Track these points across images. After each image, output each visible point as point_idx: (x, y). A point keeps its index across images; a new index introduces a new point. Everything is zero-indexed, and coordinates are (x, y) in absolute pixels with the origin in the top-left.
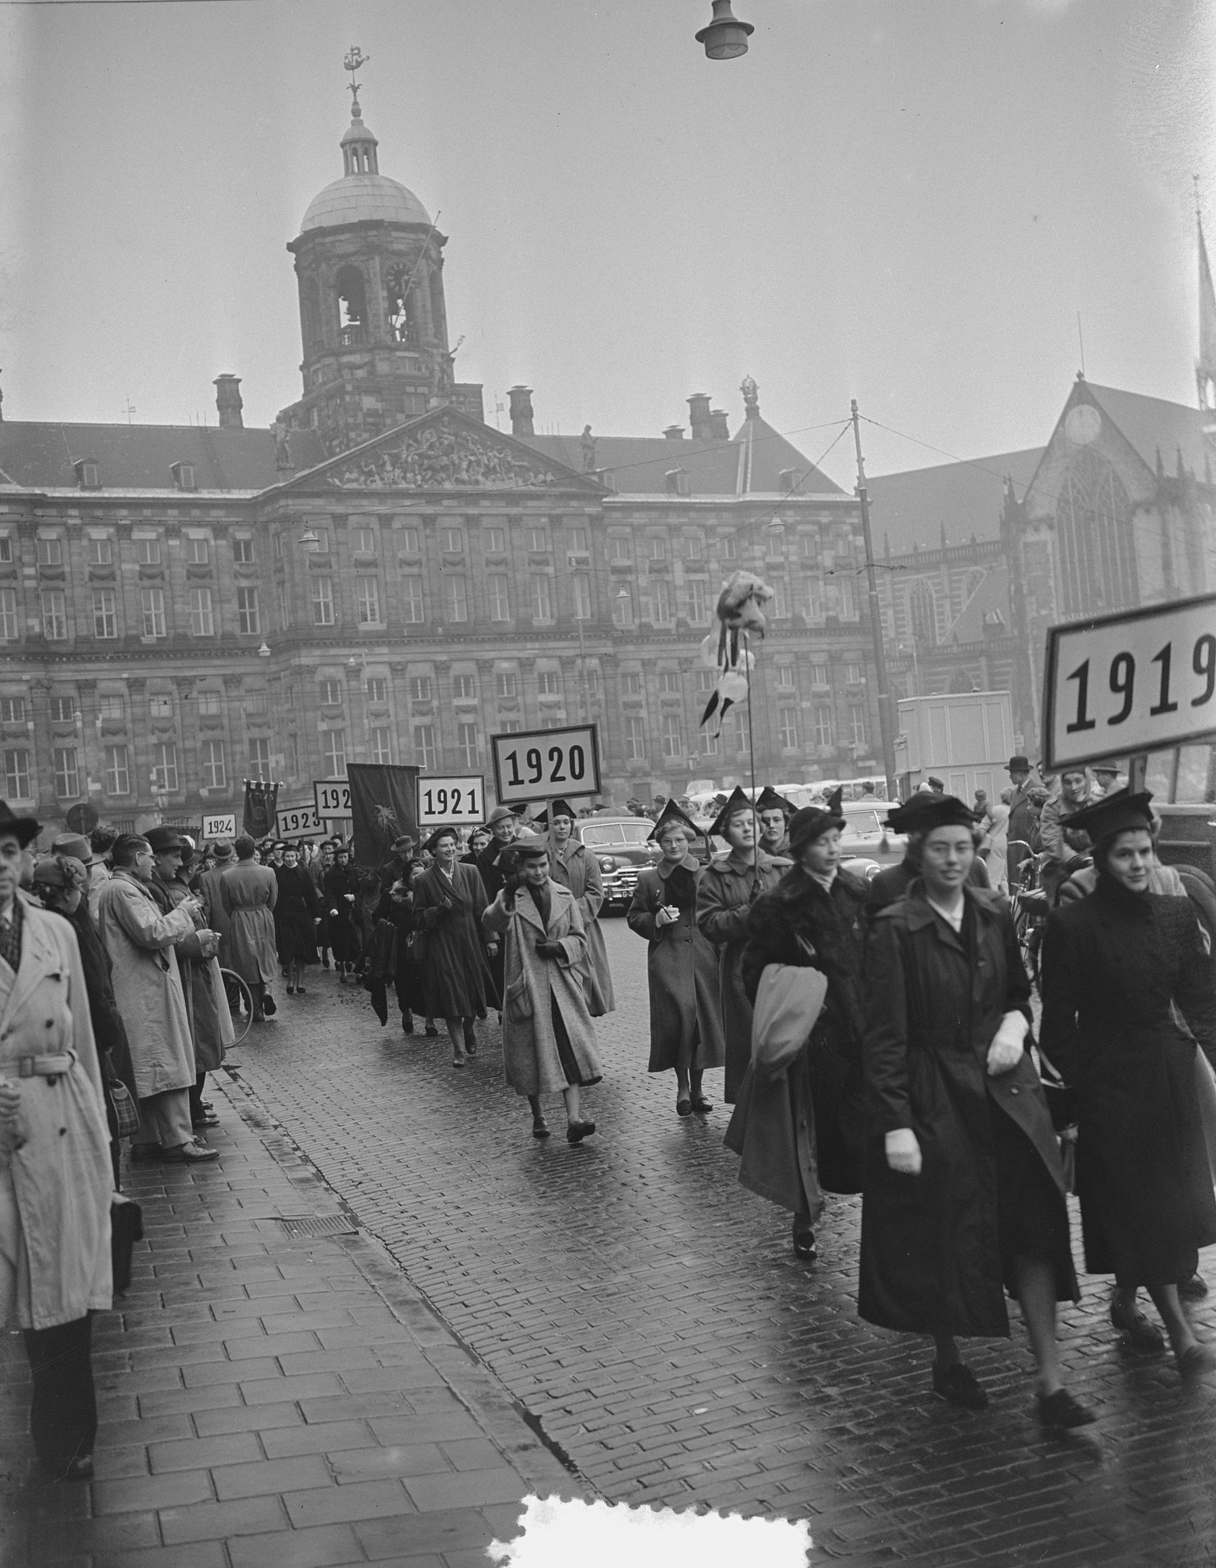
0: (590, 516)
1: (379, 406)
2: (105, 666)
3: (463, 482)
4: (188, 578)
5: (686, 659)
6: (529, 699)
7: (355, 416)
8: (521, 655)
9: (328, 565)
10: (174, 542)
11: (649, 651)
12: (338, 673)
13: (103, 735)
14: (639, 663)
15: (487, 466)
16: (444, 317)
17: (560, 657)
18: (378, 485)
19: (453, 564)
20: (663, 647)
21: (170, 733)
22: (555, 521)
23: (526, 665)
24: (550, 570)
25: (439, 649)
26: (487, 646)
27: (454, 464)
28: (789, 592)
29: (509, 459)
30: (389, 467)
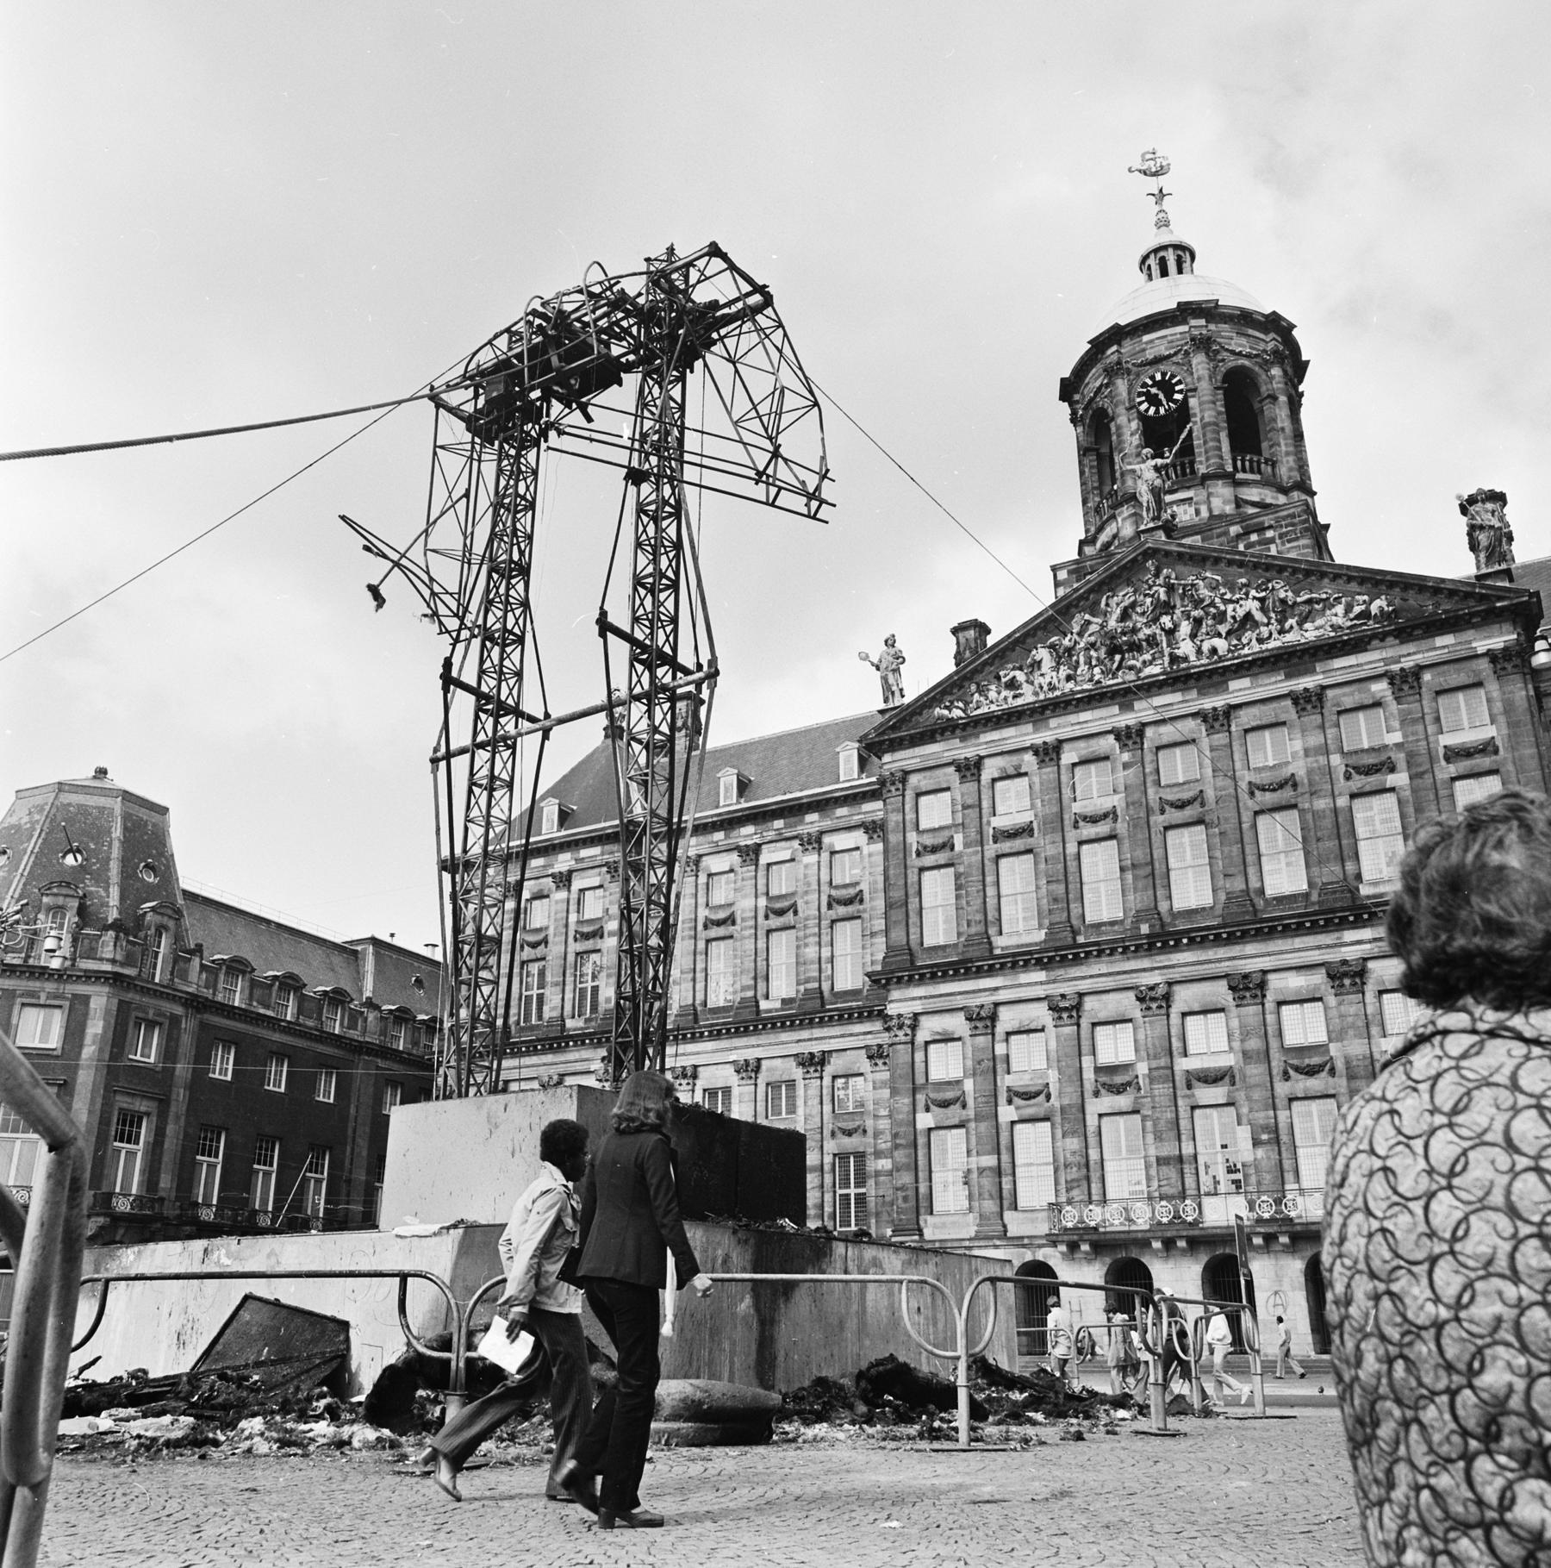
0: (1492, 656)
2: (710, 1045)
3: (1186, 659)
4: (830, 907)
6: (1357, 1048)
9: (948, 845)
10: (812, 858)
15: (1234, 617)
18: (1028, 697)
19: (1181, 805)
22: (1405, 682)
23: (1348, 977)
24: (1400, 779)
25: (1146, 963)
26: (1250, 949)
29: (1282, 595)
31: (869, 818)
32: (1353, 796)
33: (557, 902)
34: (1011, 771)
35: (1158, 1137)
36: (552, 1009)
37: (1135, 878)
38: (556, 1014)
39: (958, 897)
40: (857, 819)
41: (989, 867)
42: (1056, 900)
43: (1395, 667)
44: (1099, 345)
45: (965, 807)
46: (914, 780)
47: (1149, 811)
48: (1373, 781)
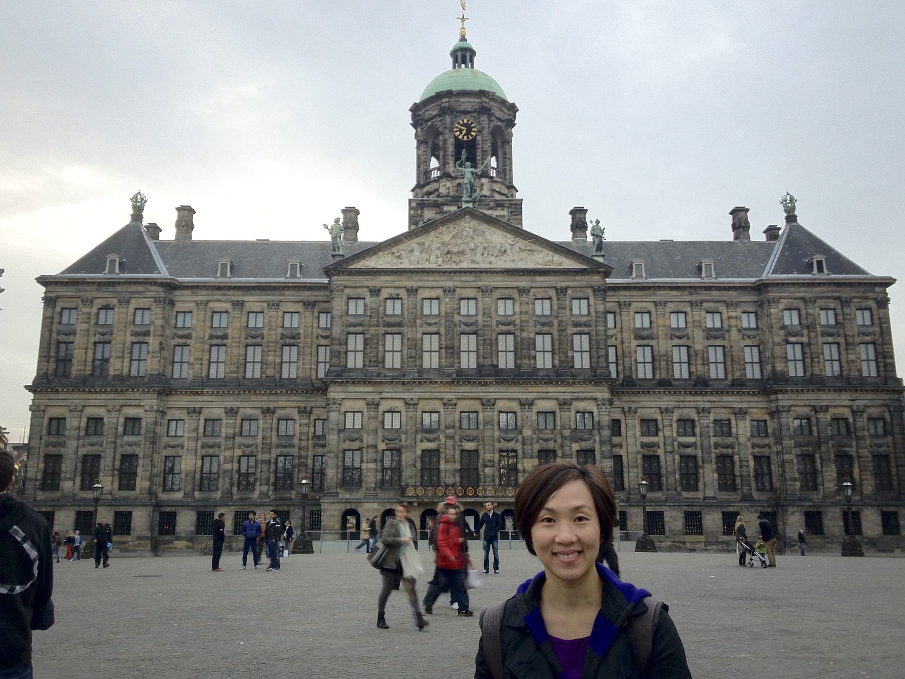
1: (438, 217)
2: (210, 398)
4: (282, 338)
5: (704, 410)
7: (417, 224)
8: (523, 396)
11: (666, 401)
12: (360, 405)
13: (203, 447)
14: (658, 411)
16: (510, 159)
17: (557, 399)
20: (682, 398)
21: (253, 448)
23: (526, 404)
26: (491, 389)
27: (472, 250)
28: (808, 355)
30: (416, 253)
31: (306, 299)
32: (537, 334)
33: (120, 313)
34: (394, 296)
35: (447, 461)
36: (115, 370)
37: (446, 353)
38: (117, 373)
39: (365, 348)
40: (299, 298)
41: (381, 337)
42: (411, 357)
43: (559, 285)
44: (439, 96)
45: (371, 309)
46: (347, 291)
47: (456, 325)
48: (546, 329)
